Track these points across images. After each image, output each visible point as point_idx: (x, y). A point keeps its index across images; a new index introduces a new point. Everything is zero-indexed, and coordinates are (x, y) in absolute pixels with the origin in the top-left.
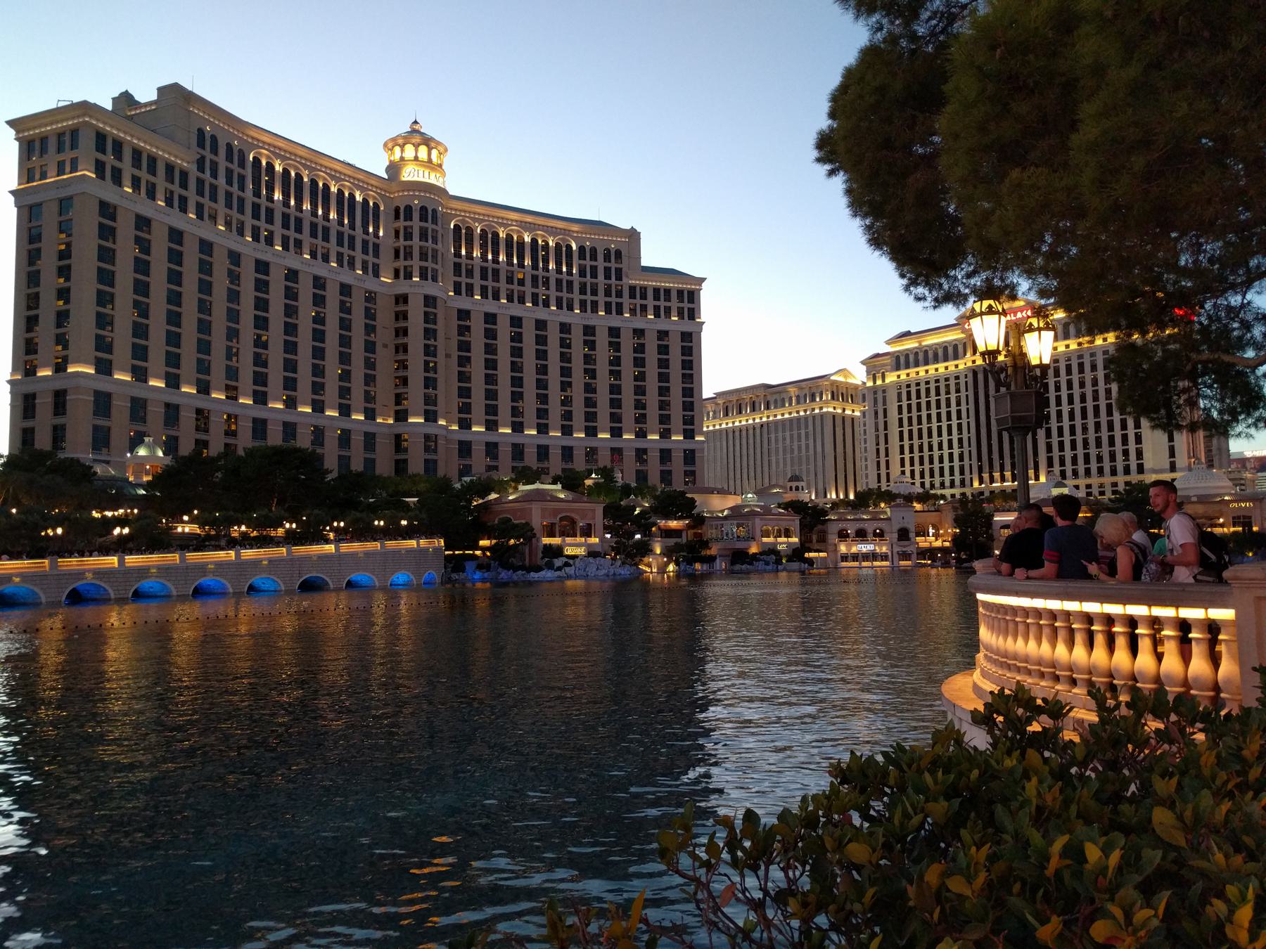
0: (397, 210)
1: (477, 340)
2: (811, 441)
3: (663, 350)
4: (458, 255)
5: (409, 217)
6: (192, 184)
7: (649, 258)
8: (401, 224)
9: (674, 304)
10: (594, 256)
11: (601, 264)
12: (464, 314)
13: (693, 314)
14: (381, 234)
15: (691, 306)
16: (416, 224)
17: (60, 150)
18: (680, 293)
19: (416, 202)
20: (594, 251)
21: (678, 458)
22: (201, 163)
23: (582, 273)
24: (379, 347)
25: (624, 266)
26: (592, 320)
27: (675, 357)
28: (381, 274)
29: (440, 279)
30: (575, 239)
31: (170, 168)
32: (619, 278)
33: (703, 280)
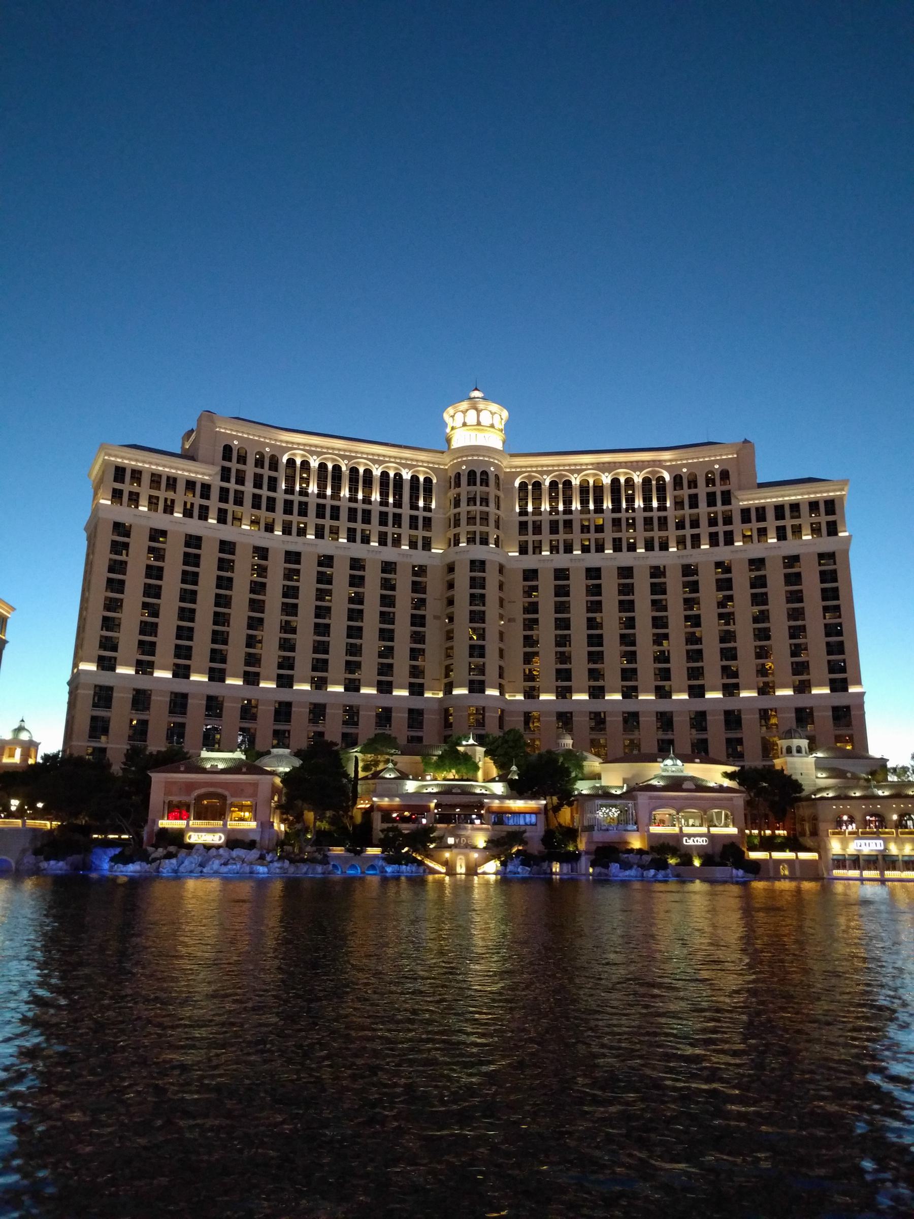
1: (546, 598)
4: (524, 512)
6: (215, 494)
8: (452, 493)
9: (806, 519)
10: (693, 483)
11: (702, 491)
12: (531, 574)
14: (433, 506)
16: (464, 489)
18: (814, 506)
19: (464, 467)
22: (225, 474)
23: (678, 504)
24: (429, 620)
26: (691, 556)
27: (812, 586)
28: (433, 545)
29: (491, 541)
30: (667, 468)
31: (190, 485)
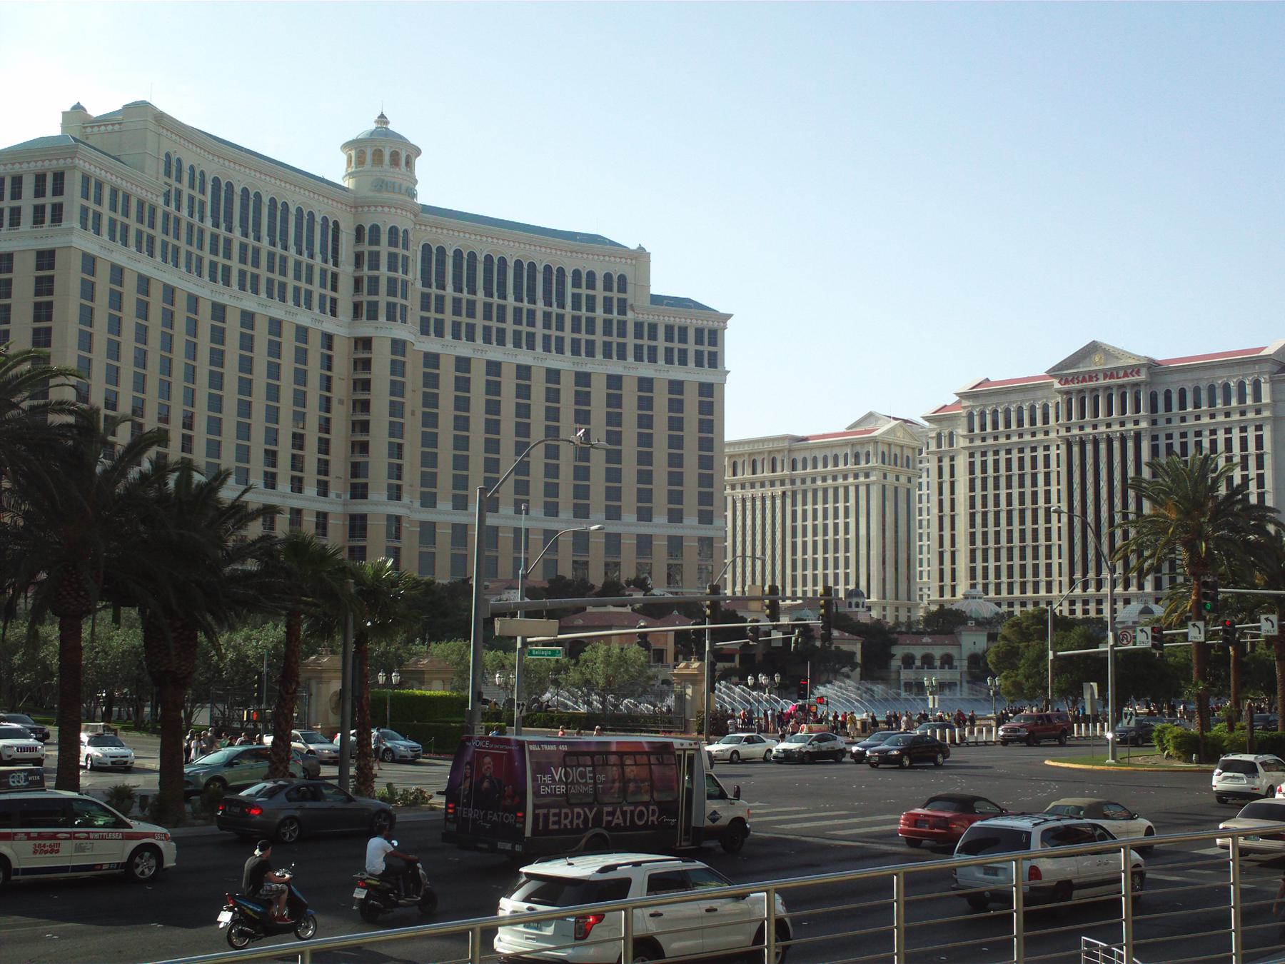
0: (359, 230)
2: (852, 521)
3: (676, 406)
5: (375, 240)
7: (661, 284)
12: (432, 360)
13: (714, 360)
15: (712, 349)
17: (40, 192)
18: (699, 332)
20: (591, 275)
21: (691, 547)
22: (167, 196)
24: (334, 404)
25: (629, 296)
31: (141, 204)
32: (622, 311)
33: (730, 316)
